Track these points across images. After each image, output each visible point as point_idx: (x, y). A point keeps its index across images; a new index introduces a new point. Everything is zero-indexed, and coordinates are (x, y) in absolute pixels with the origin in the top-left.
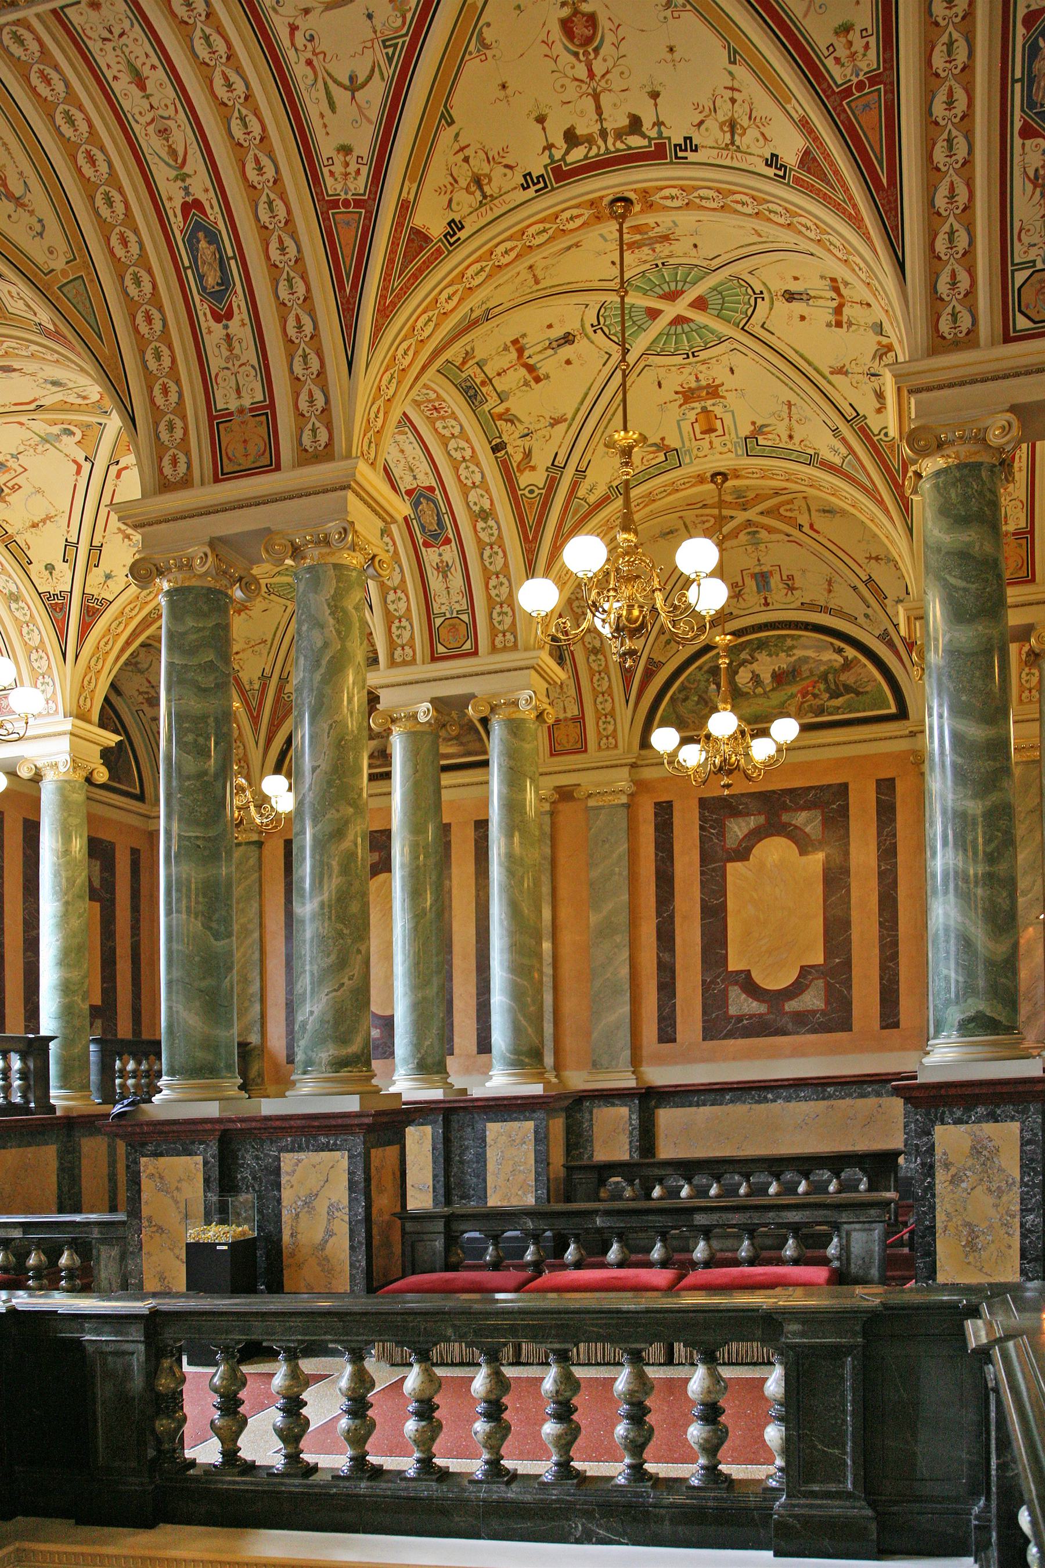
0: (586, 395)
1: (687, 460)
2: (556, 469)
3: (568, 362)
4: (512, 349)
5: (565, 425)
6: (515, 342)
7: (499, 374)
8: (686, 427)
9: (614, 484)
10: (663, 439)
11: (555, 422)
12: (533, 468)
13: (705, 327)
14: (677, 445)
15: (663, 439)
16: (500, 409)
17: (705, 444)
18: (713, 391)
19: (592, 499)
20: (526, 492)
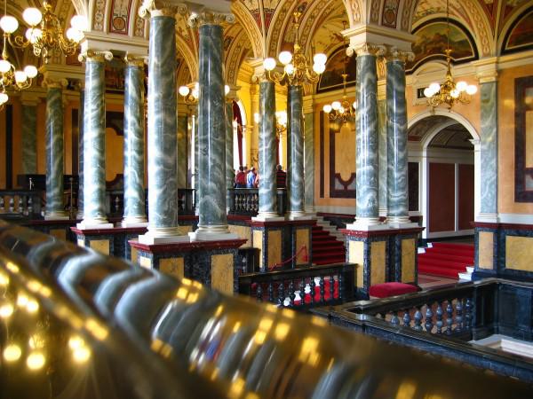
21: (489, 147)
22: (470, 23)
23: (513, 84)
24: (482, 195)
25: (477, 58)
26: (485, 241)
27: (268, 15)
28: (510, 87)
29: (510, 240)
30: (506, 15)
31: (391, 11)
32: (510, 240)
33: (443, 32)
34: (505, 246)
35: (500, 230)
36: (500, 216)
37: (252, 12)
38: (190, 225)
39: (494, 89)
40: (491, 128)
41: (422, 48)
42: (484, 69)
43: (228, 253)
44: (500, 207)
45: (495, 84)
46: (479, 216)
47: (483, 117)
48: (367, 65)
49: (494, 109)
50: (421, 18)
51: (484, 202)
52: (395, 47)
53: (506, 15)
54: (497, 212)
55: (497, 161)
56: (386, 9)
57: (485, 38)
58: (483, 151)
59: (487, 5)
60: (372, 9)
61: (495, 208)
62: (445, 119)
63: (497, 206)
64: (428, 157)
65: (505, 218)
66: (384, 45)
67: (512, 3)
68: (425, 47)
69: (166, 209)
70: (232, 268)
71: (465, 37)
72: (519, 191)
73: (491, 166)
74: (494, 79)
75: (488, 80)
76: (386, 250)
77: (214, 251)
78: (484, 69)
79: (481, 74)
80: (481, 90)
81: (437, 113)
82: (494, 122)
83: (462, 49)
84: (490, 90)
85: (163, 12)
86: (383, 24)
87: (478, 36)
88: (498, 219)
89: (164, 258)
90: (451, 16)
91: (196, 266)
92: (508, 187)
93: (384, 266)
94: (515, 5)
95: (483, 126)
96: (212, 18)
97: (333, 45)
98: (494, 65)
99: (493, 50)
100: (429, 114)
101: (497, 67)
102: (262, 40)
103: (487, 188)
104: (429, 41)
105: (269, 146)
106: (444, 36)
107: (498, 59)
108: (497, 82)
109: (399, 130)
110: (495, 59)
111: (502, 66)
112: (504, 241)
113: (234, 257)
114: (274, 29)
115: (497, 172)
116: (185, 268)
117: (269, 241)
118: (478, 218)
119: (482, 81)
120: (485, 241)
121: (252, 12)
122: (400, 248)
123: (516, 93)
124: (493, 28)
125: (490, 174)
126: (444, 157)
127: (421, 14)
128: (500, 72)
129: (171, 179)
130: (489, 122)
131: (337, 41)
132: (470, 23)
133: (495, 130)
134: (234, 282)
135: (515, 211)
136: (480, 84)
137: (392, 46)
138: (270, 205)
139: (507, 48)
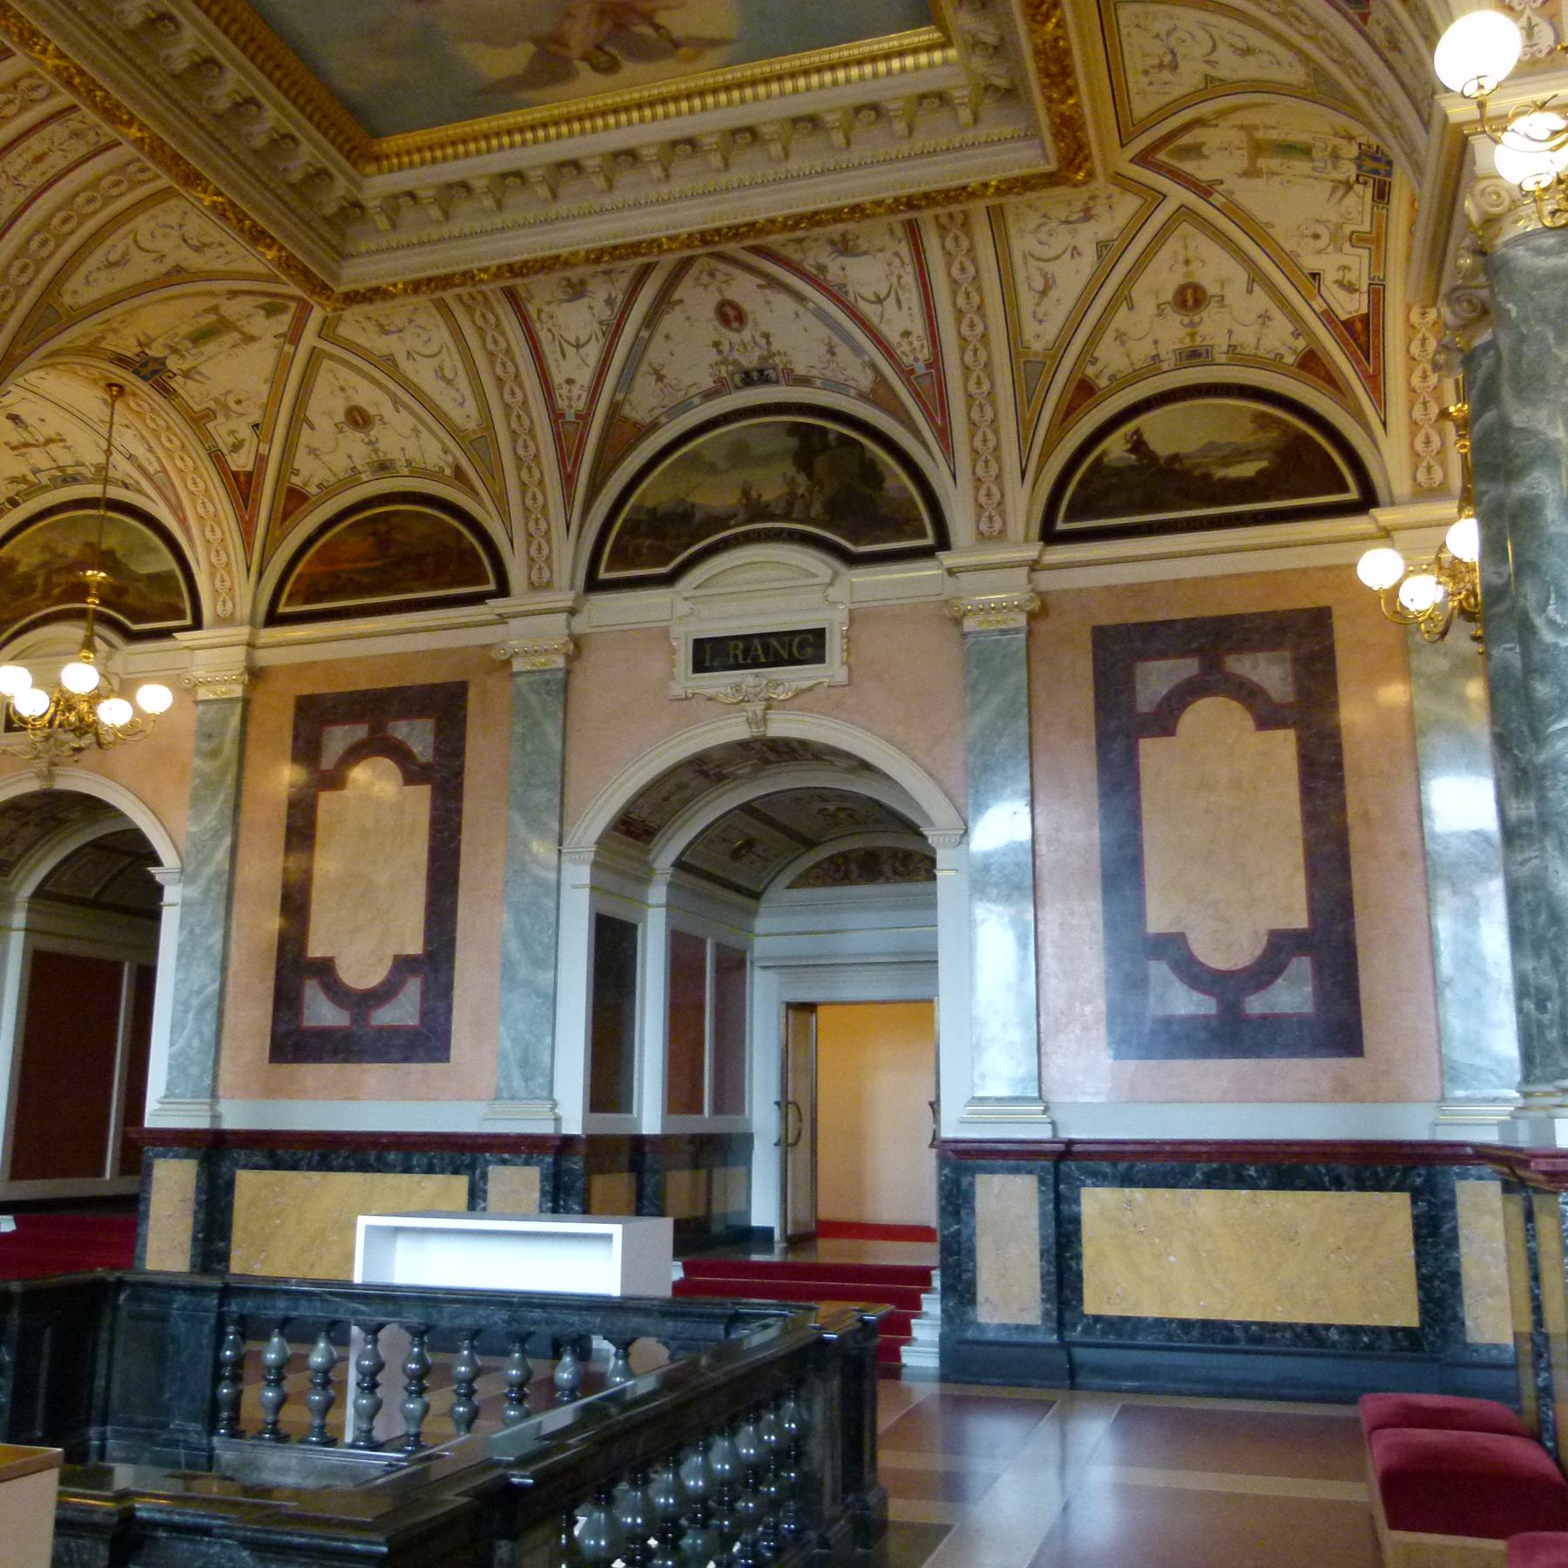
21: (207, 890)
22: (183, 522)
23: (290, 712)
24: (172, 1044)
25: (197, 624)
26: (172, 1186)
28: (278, 721)
29: (249, 1184)
30: (286, 515)
32: (249, 1184)
33: (111, 541)
34: (230, 1205)
35: (217, 1152)
36: (224, 1107)
39: (235, 721)
40: (217, 834)
41: (40, 581)
42: (212, 657)
44: (225, 1078)
45: (238, 709)
46: (158, 1112)
47: (196, 801)
49: (230, 779)
50: (44, 489)
51: (177, 1066)
53: (286, 515)
54: (214, 1095)
55: (226, 937)
57: (225, 572)
58: (186, 905)
59: (235, 475)
61: (208, 1081)
62: (94, 807)
63: (215, 1077)
64: (28, 930)
65: (236, 1116)
67: (306, 484)
68: (48, 581)
71: (172, 565)
72: (283, 1028)
73: (209, 949)
74: (238, 691)
75: (222, 691)
78: (212, 657)
79: (200, 674)
80: (200, 721)
81: (63, 784)
82: (228, 822)
83: (158, 599)
84: (225, 720)
87: (203, 564)
88: (216, 1117)
90: (115, 493)
92: (252, 1017)
94: (313, 490)
95: (193, 829)
98: (239, 654)
99: (244, 610)
100: (33, 786)
101: (249, 658)
103: (191, 1015)
104: (60, 563)
106: (110, 553)
107: (252, 635)
108: (246, 702)
110: (243, 632)
111: (265, 658)
112: (230, 1186)
115: (224, 969)
118: (155, 1114)
119: (203, 694)
120: (172, 1186)
123: (296, 738)
124: (248, 545)
125: (204, 975)
126: (80, 937)
127: (44, 478)
128: (255, 674)
130: (214, 813)
132: (183, 522)
133: (227, 842)
135: (270, 1092)
136: (197, 703)
139: (283, 609)
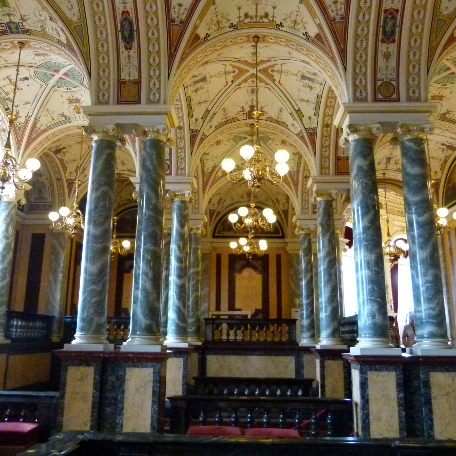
0: (36, 96)
1: (72, 121)
2: (28, 117)
3: (28, 85)
4: (7, 79)
5: (30, 105)
6: (7, 77)
7: (4, 86)
8: (71, 110)
9: (49, 125)
10: (63, 113)
11: (26, 103)
12: (20, 117)
13: (70, 82)
14: (68, 115)
15: (63, 113)
16: (7, 97)
17: (78, 116)
18: (78, 101)
19: (42, 128)
20: (18, 124)
27: (312, 134)
31: (387, 84)
37: (298, 135)
38: (292, 356)
43: (147, 367)
48: (356, 150)
52: (400, 123)
56: (379, 83)
60: (355, 87)
66: (379, 123)
69: (85, 316)
70: (151, 384)
76: (398, 385)
77: (130, 363)
85: (98, 136)
86: (376, 100)
89: (73, 365)
91: (112, 378)
93: (396, 408)
96: (145, 133)
97: (447, 157)
102: (312, 158)
105: (325, 266)
109: (417, 222)
113: (154, 372)
114: (322, 146)
116: (95, 379)
117: (326, 373)
121: (298, 135)
122: (427, 384)
129: (93, 287)
131: (450, 152)
134: (153, 402)
137: (398, 122)
138: (329, 331)
